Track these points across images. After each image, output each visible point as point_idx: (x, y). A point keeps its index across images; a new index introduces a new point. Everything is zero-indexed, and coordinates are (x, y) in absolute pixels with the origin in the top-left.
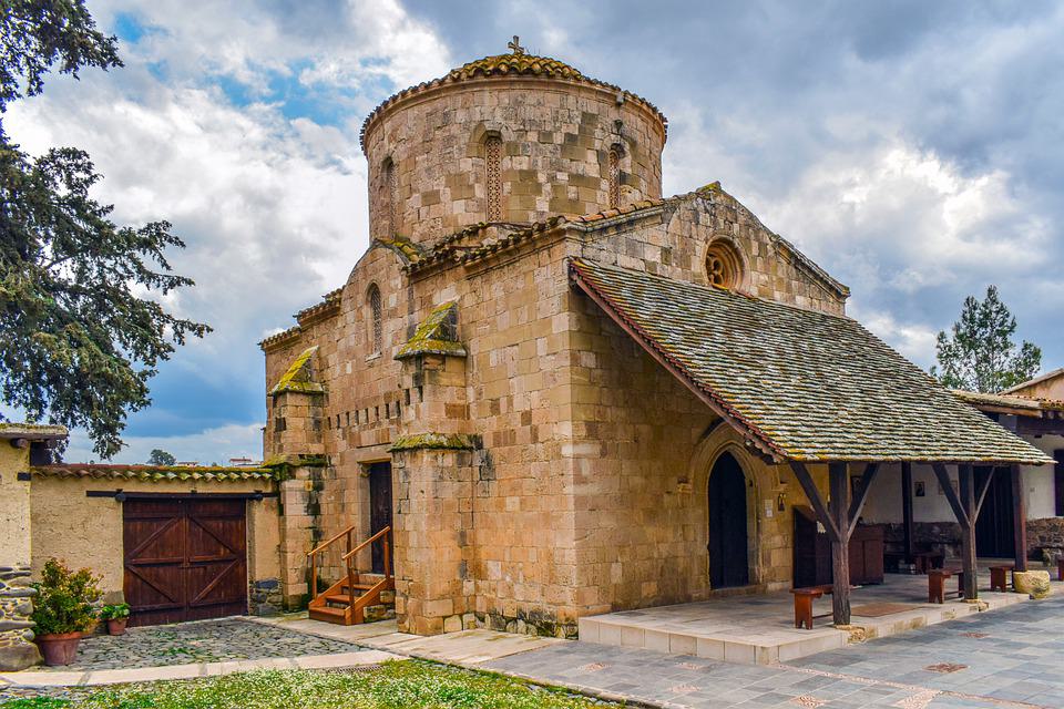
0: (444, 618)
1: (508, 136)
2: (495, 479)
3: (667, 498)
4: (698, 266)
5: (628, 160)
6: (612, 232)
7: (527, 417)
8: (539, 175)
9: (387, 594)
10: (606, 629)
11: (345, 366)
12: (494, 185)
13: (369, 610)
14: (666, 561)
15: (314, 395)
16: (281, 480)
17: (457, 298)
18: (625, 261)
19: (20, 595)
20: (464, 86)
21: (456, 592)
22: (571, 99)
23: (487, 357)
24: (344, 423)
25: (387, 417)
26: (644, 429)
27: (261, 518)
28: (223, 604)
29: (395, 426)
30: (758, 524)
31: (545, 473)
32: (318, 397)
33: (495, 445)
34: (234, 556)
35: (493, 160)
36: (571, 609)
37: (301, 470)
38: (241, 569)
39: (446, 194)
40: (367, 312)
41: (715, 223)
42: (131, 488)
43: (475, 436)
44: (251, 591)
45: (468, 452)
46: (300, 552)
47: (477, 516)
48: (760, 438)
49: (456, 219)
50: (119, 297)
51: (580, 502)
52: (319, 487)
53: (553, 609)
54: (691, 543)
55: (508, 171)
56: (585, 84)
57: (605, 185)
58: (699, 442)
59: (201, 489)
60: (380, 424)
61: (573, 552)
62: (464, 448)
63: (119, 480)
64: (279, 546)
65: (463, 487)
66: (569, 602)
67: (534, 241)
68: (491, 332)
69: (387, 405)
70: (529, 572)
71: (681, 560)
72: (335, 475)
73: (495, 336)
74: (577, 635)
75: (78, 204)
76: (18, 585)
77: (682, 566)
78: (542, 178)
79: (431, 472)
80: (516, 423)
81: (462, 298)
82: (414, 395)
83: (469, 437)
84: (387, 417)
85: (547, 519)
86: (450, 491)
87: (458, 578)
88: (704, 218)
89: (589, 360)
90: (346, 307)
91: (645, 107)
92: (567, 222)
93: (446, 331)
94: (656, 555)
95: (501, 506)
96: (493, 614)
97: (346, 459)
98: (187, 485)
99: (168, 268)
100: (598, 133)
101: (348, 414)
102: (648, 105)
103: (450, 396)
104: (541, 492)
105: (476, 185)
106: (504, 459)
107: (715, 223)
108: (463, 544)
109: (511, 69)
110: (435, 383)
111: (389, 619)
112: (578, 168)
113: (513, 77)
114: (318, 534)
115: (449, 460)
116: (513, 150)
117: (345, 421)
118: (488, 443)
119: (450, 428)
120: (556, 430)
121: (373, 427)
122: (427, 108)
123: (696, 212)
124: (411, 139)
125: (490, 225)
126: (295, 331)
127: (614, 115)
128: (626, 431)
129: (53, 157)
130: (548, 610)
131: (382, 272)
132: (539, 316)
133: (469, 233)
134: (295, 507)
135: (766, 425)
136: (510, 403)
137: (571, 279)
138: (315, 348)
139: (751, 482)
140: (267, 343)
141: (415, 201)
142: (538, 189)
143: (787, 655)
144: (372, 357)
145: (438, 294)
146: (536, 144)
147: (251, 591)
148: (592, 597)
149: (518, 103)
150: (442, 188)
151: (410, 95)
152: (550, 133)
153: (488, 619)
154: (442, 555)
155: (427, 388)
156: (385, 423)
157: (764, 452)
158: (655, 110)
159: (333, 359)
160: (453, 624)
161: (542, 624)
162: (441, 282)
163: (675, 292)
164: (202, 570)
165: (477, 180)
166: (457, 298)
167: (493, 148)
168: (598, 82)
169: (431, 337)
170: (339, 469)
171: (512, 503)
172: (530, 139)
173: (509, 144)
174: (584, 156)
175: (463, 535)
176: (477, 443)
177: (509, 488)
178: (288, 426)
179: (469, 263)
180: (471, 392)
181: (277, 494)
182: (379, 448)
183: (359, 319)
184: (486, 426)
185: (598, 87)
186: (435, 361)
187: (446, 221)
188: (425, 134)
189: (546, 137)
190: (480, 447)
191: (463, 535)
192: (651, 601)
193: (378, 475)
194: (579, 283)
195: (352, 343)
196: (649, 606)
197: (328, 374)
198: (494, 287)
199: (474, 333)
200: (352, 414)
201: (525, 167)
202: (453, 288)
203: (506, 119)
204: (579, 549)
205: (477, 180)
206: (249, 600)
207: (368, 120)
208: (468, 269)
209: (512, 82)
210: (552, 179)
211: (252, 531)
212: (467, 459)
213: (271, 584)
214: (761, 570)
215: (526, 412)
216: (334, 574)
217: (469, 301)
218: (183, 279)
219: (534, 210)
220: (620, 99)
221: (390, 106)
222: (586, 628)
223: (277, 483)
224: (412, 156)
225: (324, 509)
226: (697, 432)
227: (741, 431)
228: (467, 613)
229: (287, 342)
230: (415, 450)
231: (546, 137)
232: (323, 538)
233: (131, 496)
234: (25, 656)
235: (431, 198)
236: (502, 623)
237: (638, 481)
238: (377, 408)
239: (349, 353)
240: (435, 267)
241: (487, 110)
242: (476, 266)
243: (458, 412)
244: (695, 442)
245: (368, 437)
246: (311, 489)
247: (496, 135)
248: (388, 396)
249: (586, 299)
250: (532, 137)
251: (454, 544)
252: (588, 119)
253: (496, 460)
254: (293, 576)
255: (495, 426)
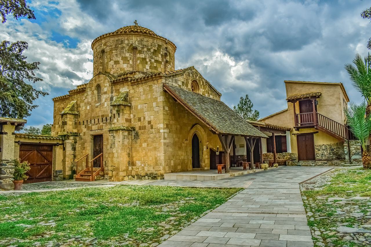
0: (124, 176)
1: (139, 49)
2: (139, 139)
3: (183, 144)
4: (190, 86)
5: (168, 57)
6: (172, 77)
7: (149, 122)
8: (147, 59)
9: (101, 172)
10: (174, 176)
11: (87, 107)
12: (135, 61)
13: (97, 177)
14: (183, 161)
15: (75, 115)
16: (65, 140)
17: (128, 90)
18: (175, 84)
19: (11, 168)
20: (127, 34)
21: (127, 170)
22: (155, 41)
23: (137, 106)
24: (85, 123)
25: (102, 122)
26: (178, 126)
27: (58, 151)
28: (45, 178)
29: (105, 124)
30: (202, 152)
31: (155, 137)
32: (76, 116)
33: (139, 130)
34: (49, 163)
35: (135, 54)
36: (162, 172)
37: (71, 137)
38: (51, 167)
39: (121, 62)
40: (96, 92)
41: (193, 76)
42: (22, 140)
43: (133, 127)
44: (54, 174)
45: (131, 131)
46: (70, 162)
47: (133, 149)
48: (213, 128)
49: (124, 69)
50: (20, 83)
51: (165, 144)
52: (76, 142)
53: (157, 172)
54: (186, 155)
55: (139, 57)
56: (159, 38)
57: (163, 63)
58: (190, 130)
59: (42, 142)
60: (99, 124)
61: (163, 157)
62: (130, 130)
63: (19, 138)
64: (63, 160)
65: (129, 141)
66: (161, 170)
67: (153, 78)
68: (139, 100)
69: (102, 119)
70: (149, 163)
71: (186, 160)
72: (81, 139)
73: (140, 101)
74: (164, 178)
75: (17, 56)
76: (10, 165)
77: (186, 162)
78: (148, 60)
79: (122, 136)
80: (146, 124)
81: (130, 90)
82: (117, 116)
83: (131, 127)
84: (102, 122)
85: (155, 149)
86: (126, 142)
87: (128, 166)
88: (191, 75)
89: (167, 108)
90: (88, 90)
91: (172, 44)
92: (163, 74)
93: (125, 99)
94: (181, 159)
95: (141, 146)
96: (137, 175)
97: (86, 134)
98: (38, 140)
99: (34, 75)
100: (162, 50)
101: (87, 121)
102: (173, 44)
103: (126, 116)
104: (153, 142)
105: (130, 60)
106: (142, 133)
107: (193, 76)
108: (129, 156)
109: (141, 32)
110: (123, 113)
111: (102, 180)
112: (157, 58)
113: (141, 34)
114: (75, 156)
115: (126, 133)
116: (140, 52)
117: (86, 123)
118: (137, 129)
119: (126, 125)
120: (158, 126)
121: (97, 125)
122: (117, 38)
123: (189, 73)
124: (111, 46)
125: (136, 72)
126: (68, 96)
127: (165, 46)
128: (174, 126)
129: (18, 43)
130: (155, 173)
131: (102, 81)
132: (154, 97)
133: (130, 73)
134: (69, 148)
135: (214, 125)
136: (144, 118)
137: (163, 88)
138: (76, 101)
139: (201, 141)
140: (55, 99)
141: (112, 63)
142: (147, 63)
143: (219, 178)
144: (97, 105)
145: (121, 89)
146: (146, 51)
147: (54, 174)
148: (167, 168)
149: (142, 40)
150: (120, 60)
151: (111, 34)
152: (150, 49)
153: (136, 177)
154: (124, 159)
155: (121, 114)
156: (101, 124)
157: (214, 131)
158: (174, 45)
159: (82, 105)
160: (126, 178)
161: (153, 176)
162: (122, 86)
163: (186, 93)
164: (39, 167)
165: (130, 59)
166: (128, 90)
167: (135, 51)
168: (162, 37)
169: (122, 100)
170: (83, 137)
171: (144, 145)
172: (145, 50)
173: (139, 51)
174: (158, 55)
175: (129, 154)
176: (133, 129)
177: (143, 141)
178: (67, 124)
179: (132, 81)
180: (132, 116)
181: (63, 144)
182: (99, 131)
183: (93, 94)
184: (137, 125)
185: (162, 38)
186: (123, 107)
187: (121, 69)
188: (116, 45)
189: (149, 50)
190: (134, 130)
191: (129, 154)
192: (180, 171)
193: (98, 139)
194: (166, 89)
195: (90, 100)
196: (179, 172)
197: (80, 109)
198: (140, 88)
199: (133, 100)
200: (89, 121)
201: (143, 57)
202: (127, 88)
203: (139, 44)
204: (164, 156)
205: (130, 59)
206: (52, 176)
207: (96, 39)
208: (132, 83)
209: (141, 35)
210: (150, 61)
211: (55, 155)
212: (131, 133)
213: (60, 171)
214: (203, 164)
215: (149, 121)
216: (82, 168)
217: (132, 91)
218: (40, 79)
219: (145, 68)
220: (167, 42)
221: (105, 36)
222: (166, 177)
223: (63, 141)
224: (111, 50)
225: (77, 149)
226: (189, 128)
227: (208, 126)
228: (130, 175)
229: (64, 99)
230: (117, 131)
231: (149, 50)
232: (76, 157)
233: (22, 143)
234: (11, 186)
235: (117, 62)
236: (140, 177)
237: (177, 139)
238: (98, 119)
239: (89, 103)
240: (121, 82)
241: (133, 41)
242: (135, 82)
243: (128, 120)
244: (189, 130)
245: (94, 127)
246: (73, 143)
247: (136, 48)
248: (103, 116)
249: (167, 92)
250: (145, 49)
251: (127, 156)
252: (159, 46)
253: (140, 133)
254: (67, 169)
255: (140, 124)
